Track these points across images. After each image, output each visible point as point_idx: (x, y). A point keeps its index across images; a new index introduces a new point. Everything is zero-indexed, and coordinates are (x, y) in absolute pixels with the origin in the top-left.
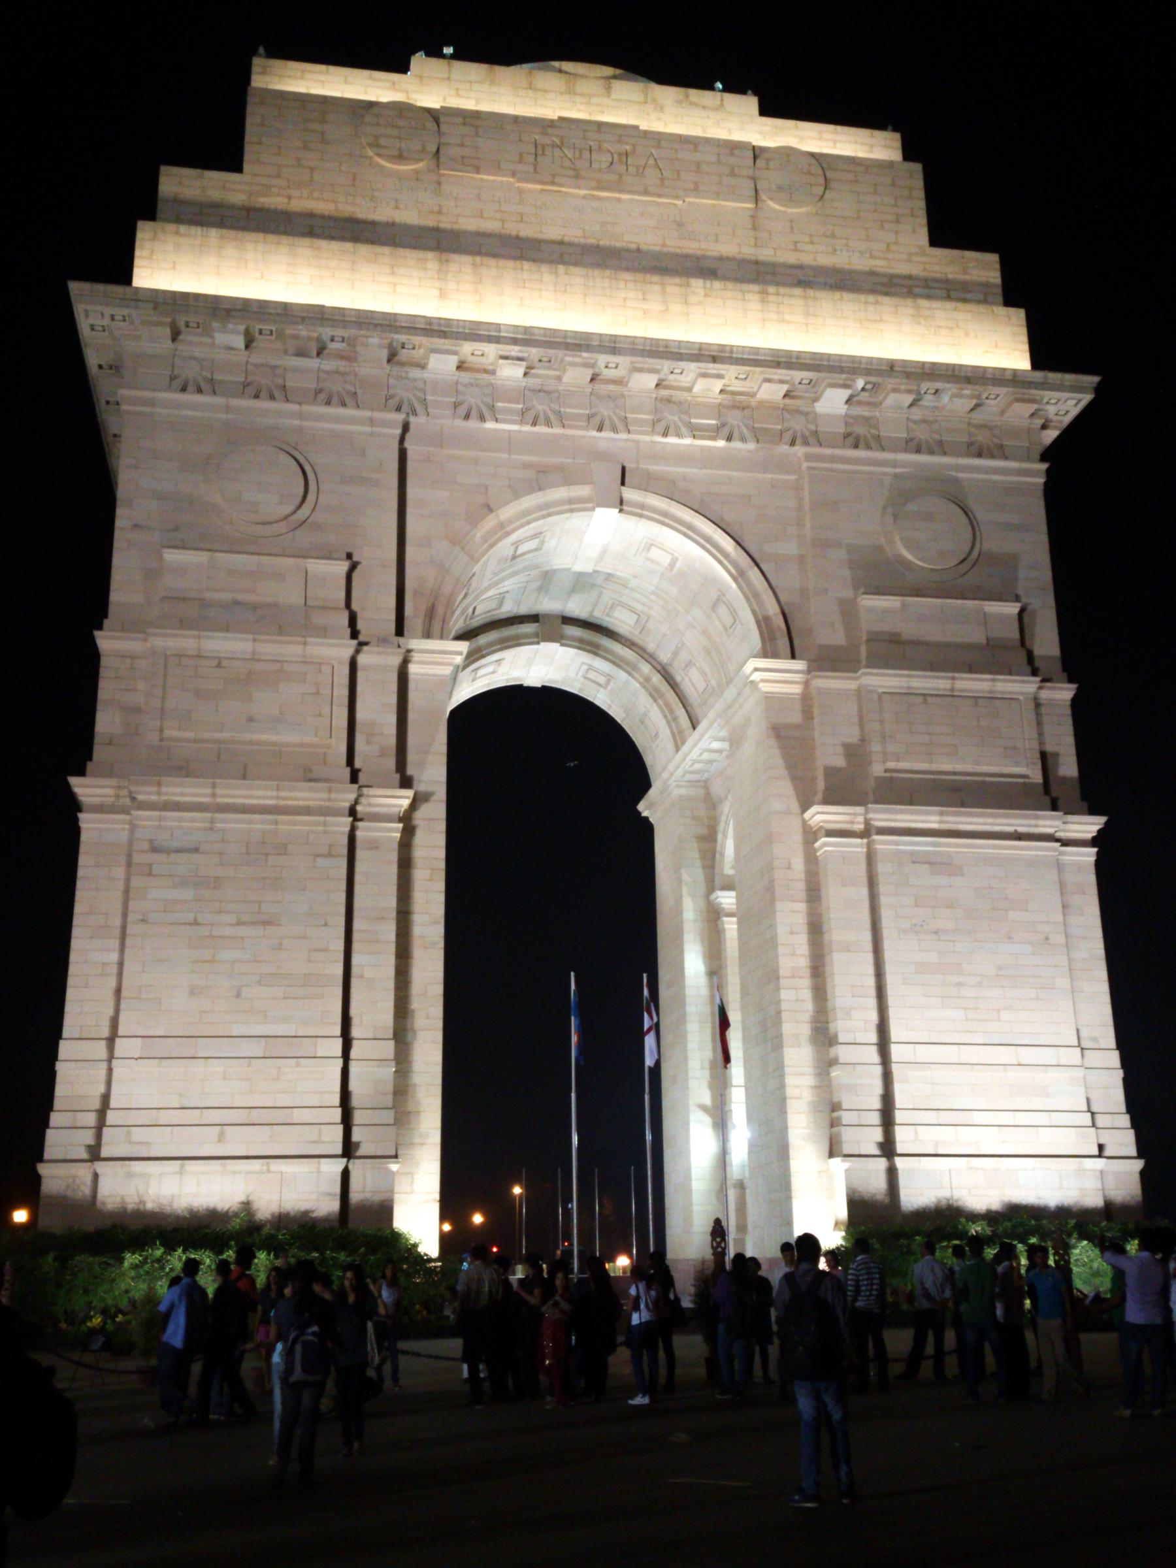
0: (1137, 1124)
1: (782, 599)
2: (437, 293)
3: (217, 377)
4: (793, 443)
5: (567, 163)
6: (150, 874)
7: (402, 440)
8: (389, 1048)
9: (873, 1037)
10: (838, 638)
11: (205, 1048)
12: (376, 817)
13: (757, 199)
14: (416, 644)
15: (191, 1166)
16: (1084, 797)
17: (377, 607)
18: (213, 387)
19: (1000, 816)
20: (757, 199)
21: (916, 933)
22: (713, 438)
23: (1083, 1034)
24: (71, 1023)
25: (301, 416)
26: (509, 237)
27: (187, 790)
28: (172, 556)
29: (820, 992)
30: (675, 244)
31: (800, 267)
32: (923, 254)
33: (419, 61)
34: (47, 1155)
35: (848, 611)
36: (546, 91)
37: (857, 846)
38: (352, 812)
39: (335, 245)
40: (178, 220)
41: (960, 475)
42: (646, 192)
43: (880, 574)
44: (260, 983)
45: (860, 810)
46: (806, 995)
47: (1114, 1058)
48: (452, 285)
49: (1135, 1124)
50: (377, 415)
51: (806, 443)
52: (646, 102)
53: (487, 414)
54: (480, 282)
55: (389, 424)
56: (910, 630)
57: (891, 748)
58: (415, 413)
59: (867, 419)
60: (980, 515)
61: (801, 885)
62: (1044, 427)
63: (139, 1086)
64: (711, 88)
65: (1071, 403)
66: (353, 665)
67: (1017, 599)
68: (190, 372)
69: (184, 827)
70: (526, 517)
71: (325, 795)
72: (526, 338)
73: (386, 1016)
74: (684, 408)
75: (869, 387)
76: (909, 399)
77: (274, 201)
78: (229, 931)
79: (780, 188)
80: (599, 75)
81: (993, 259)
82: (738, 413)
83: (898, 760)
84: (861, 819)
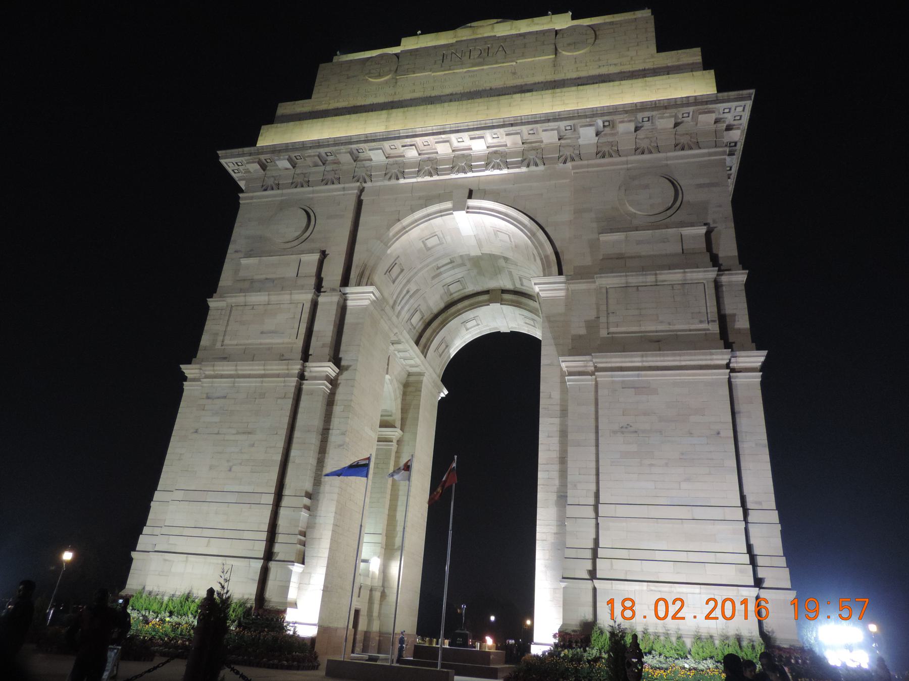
1: (557, 244)
4: (565, 162)
7: (360, 196)
9: (592, 501)
10: (588, 261)
11: (210, 497)
12: (315, 378)
13: (556, 52)
14: (348, 290)
15: (191, 557)
16: (753, 342)
17: (333, 272)
18: (278, 187)
19: (684, 355)
20: (556, 54)
21: (623, 433)
22: (519, 167)
25: (313, 192)
27: (225, 368)
28: (244, 261)
29: (563, 474)
30: (512, 82)
32: (652, 57)
33: (404, 41)
37: (588, 381)
38: (302, 377)
39: (341, 117)
40: (283, 122)
41: (669, 162)
42: (497, 63)
43: (613, 223)
44: (241, 464)
45: (588, 358)
46: (556, 475)
47: (774, 516)
49: (789, 564)
50: (347, 185)
51: (573, 160)
53: (399, 176)
55: (352, 189)
57: (612, 319)
58: (365, 182)
59: (611, 144)
60: (683, 182)
61: (558, 408)
62: (729, 128)
64: (547, 14)
65: (740, 109)
67: (705, 224)
68: (270, 182)
71: (285, 367)
75: (607, 124)
76: (631, 127)
78: (232, 438)
79: (569, 44)
81: (697, 51)
82: (534, 152)
84: (591, 364)
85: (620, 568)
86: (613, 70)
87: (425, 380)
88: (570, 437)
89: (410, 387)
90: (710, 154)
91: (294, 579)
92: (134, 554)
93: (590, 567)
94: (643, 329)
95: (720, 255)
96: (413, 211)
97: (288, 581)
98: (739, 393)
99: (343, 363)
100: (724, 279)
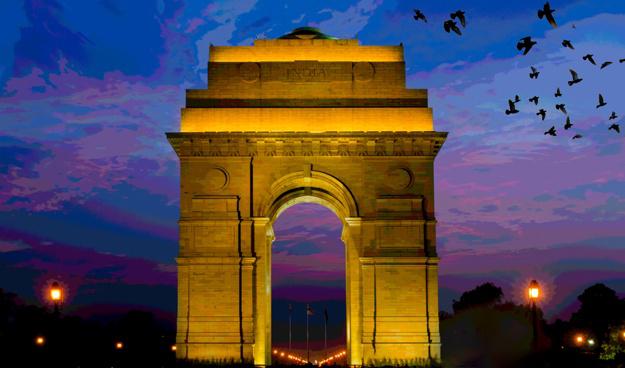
0: (441, 335)
10: (371, 211)
12: (247, 265)
13: (353, 80)
17: (245, 213)
20: (353, 80)
24: (179, 314)
28: (194, 201)
29: (361, 304)
30: (329, 96)
31: (365, 99)
37: (372, 268)
38: (241, 264)
47: (437, 319)
57: (382, 241)
59: (382, 147)
63: (195, 327)
66: (239, 226)
68: (197, 150)
72: (281, 136)
73: (250, 312)
74: (328, 147)
77: (217, 96)
85: (384, 339)
98: (430, 273)
100: (428, 224)
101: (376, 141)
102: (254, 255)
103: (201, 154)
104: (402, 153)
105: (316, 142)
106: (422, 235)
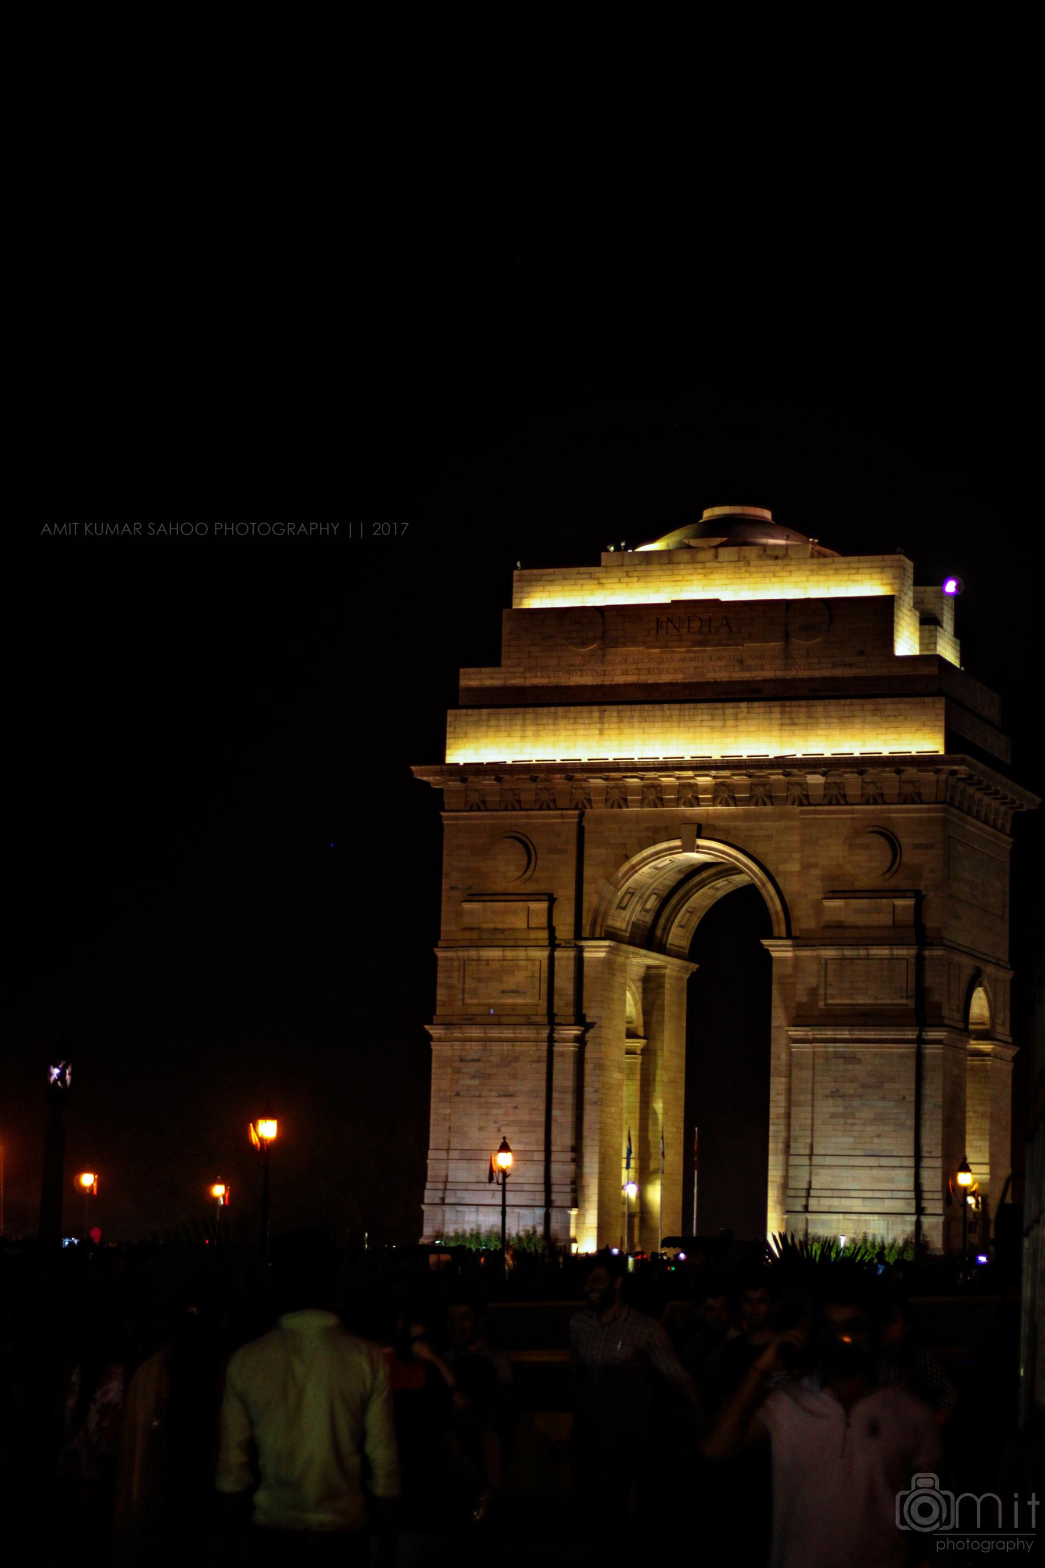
1: (787, 898)
2: (597, 732)
3: (488, 799)
5: (675, 631)
6: (460, 1072)
8: (569, 1156)
9: (807, 1152)
13: (787, 638)
14: (584, 943)
15: (482, 1209)
20: (787, 638)
23: (925, 1149)
26: (642, 684)
31: (811, 680)
34: (426, 1201)
35: (818, 908)
36: (679, 563)
37: (807, 1048)
38: (551, 1040)
46: (782, 1127)
47: (938, 1163)
48: (606, 726)
51: (801, 804)
52: (739, 561)
54: (621, 722)
55: (571, 817)
56: (850, 919)
57: (830, 992)
60: (905, 840)
61: (783, 1068)
66: (551, 959)
68: (475, 797)
69: (473, 1049)
70: (644, 861)
74: (730, 788)
80: (715, 544)
82: (762, 789)
83: (833, 998)
85: (826, 1204)
86: (848, 672)
87: (667, 971)
88: (793, 1098)
89: (651, 982)
90: (929, 811)
91: (573, 1221)
92: (423, 1207)
93: (804, 1202)
94: (854, 1002)
95: (928, 925)
96: (642, 848)
97: (569, 1222)
98: (928, 1062)
99: (588, 1020)
100: (927, 953)
101: (824, 774)
102: (580, 1019)
103: (482, 806)
104: (878, 799)
105: (704, 780)
106: (912, 979)
